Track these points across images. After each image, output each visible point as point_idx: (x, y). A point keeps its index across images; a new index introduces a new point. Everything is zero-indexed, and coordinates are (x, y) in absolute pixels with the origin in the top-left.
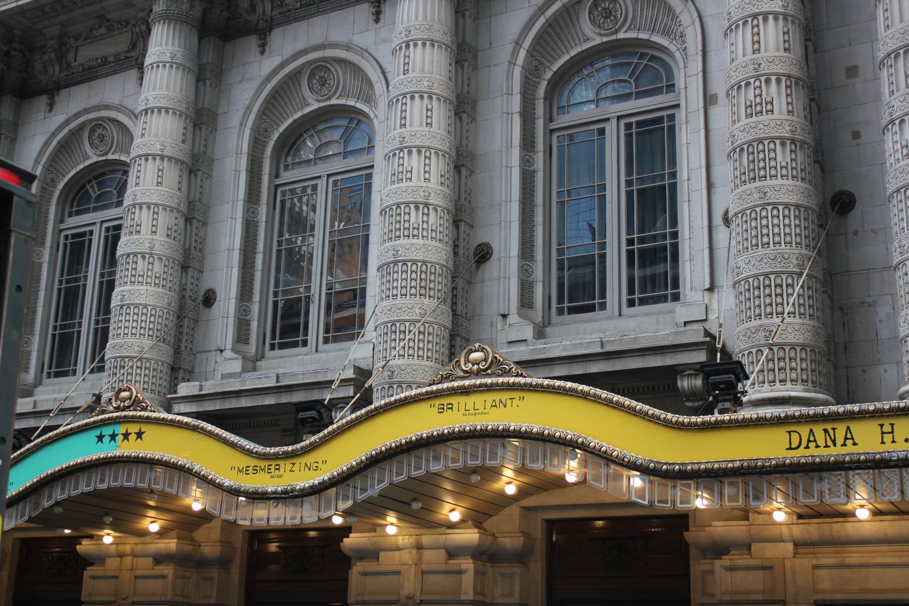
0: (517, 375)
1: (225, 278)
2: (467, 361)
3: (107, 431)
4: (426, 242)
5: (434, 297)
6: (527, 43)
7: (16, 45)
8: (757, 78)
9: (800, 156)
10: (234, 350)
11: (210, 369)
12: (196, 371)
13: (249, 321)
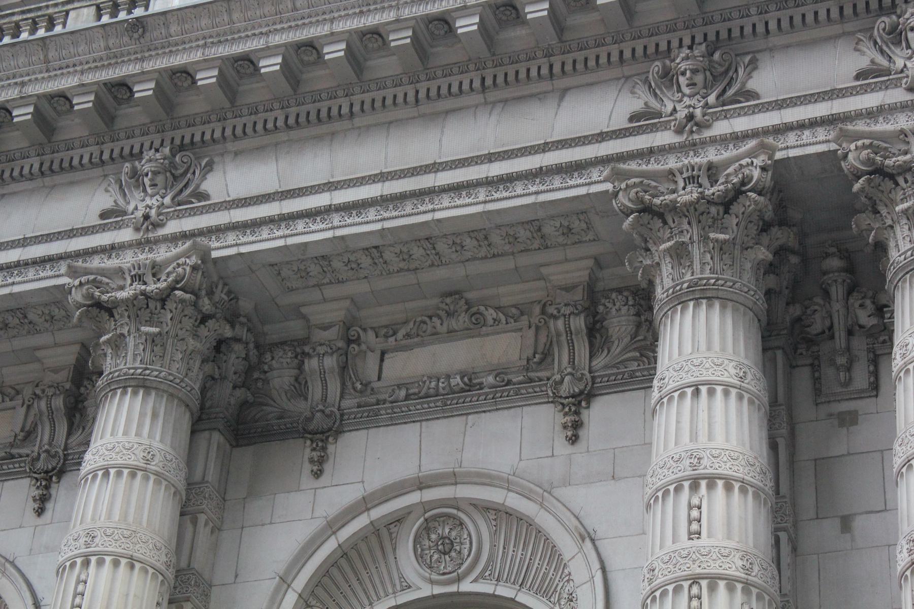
6: (301, 582)
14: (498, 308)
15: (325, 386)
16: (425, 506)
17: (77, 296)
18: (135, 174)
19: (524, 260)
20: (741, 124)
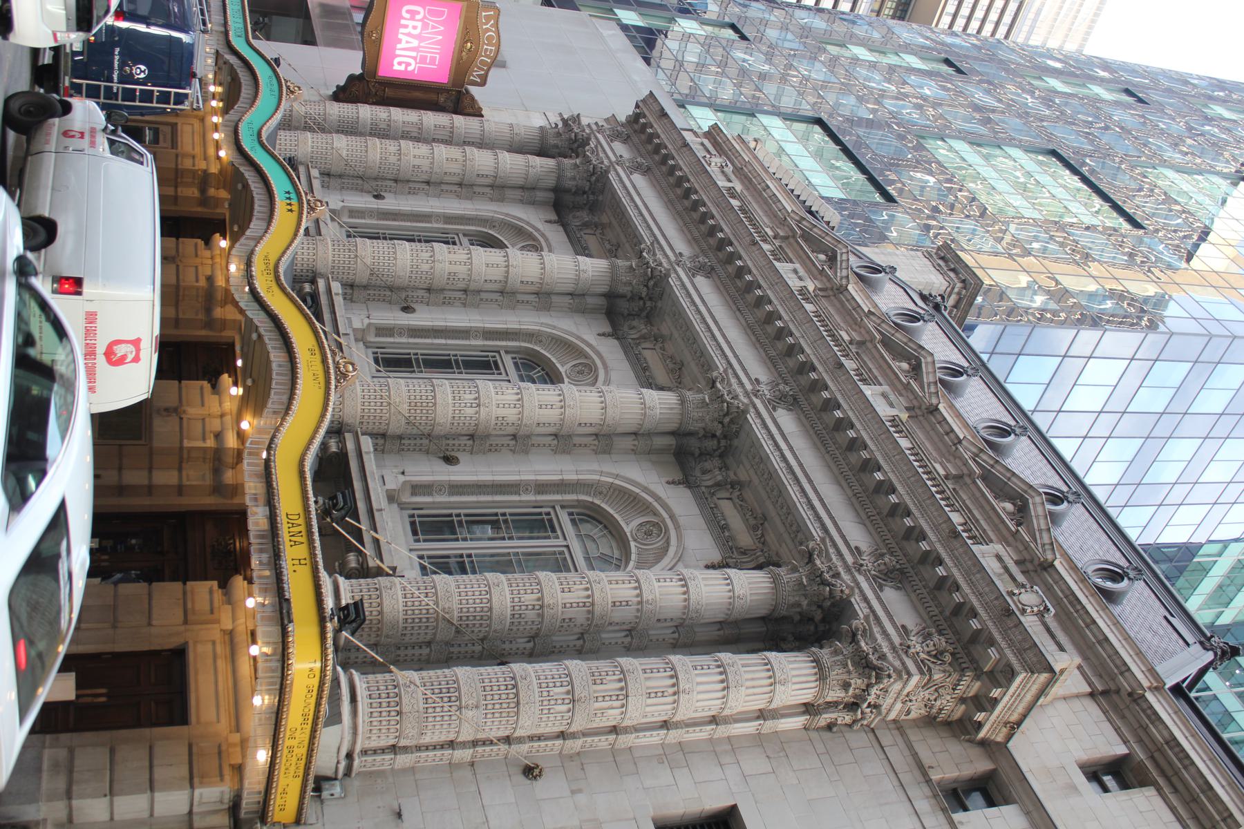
1: (423, 317)
3: (293, 196)
6: (617, 482)
7: (591, 197)
8: (589, 582)
9: (531, 615)
10: (369, 324)
14: (763, 535)
15: (708, 480)
16: (663, 521)
17: (715, 374)
18: (778, 385)
19: (786, 536)
20: (865, 585)
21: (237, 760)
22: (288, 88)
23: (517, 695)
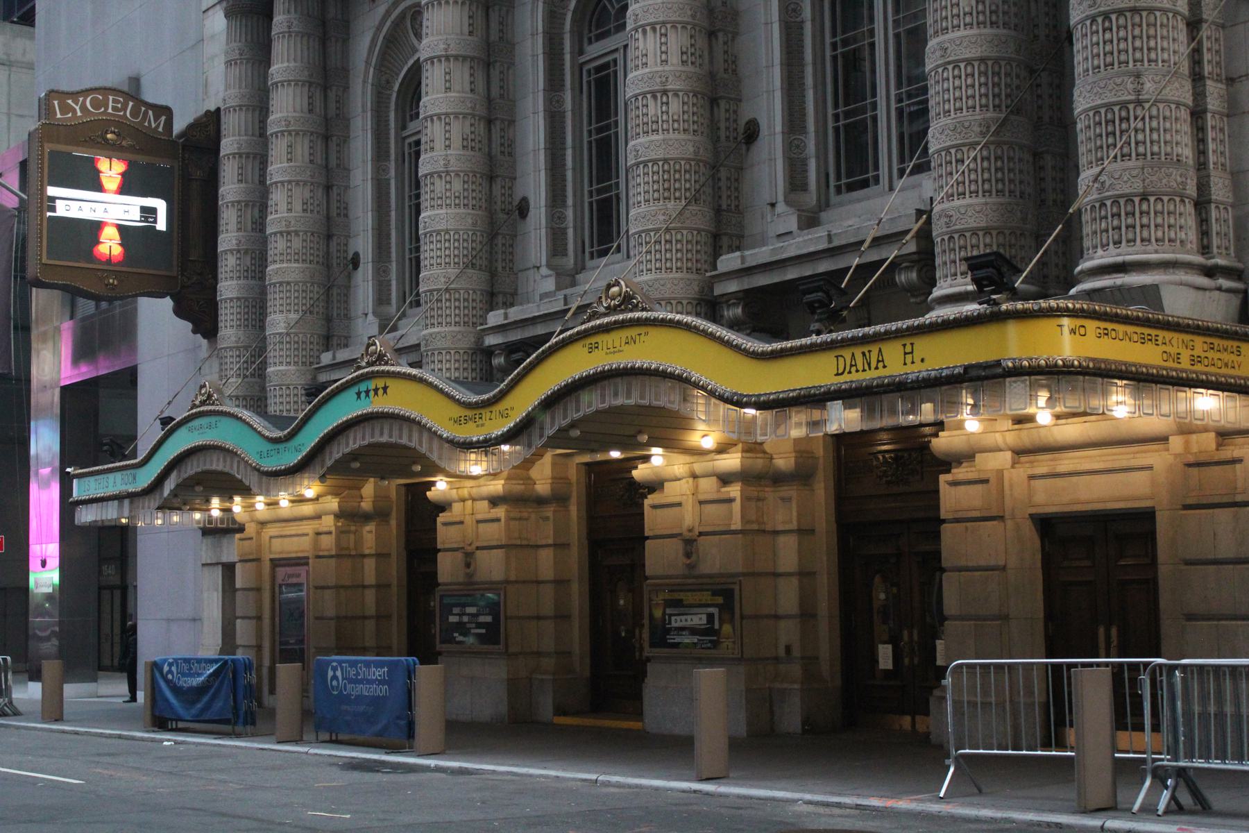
0: (644, 309)
1: (534, 183)
2: (607, 297)
3: (363, 387)
4: (667, 136)
5: (680, 199)
10: (549, 266)
11: (530, 289)
12: (520, 292)
13: (566, 228)
21: (1209, 440)
22: (203, 403)
23: (1120, 12)
